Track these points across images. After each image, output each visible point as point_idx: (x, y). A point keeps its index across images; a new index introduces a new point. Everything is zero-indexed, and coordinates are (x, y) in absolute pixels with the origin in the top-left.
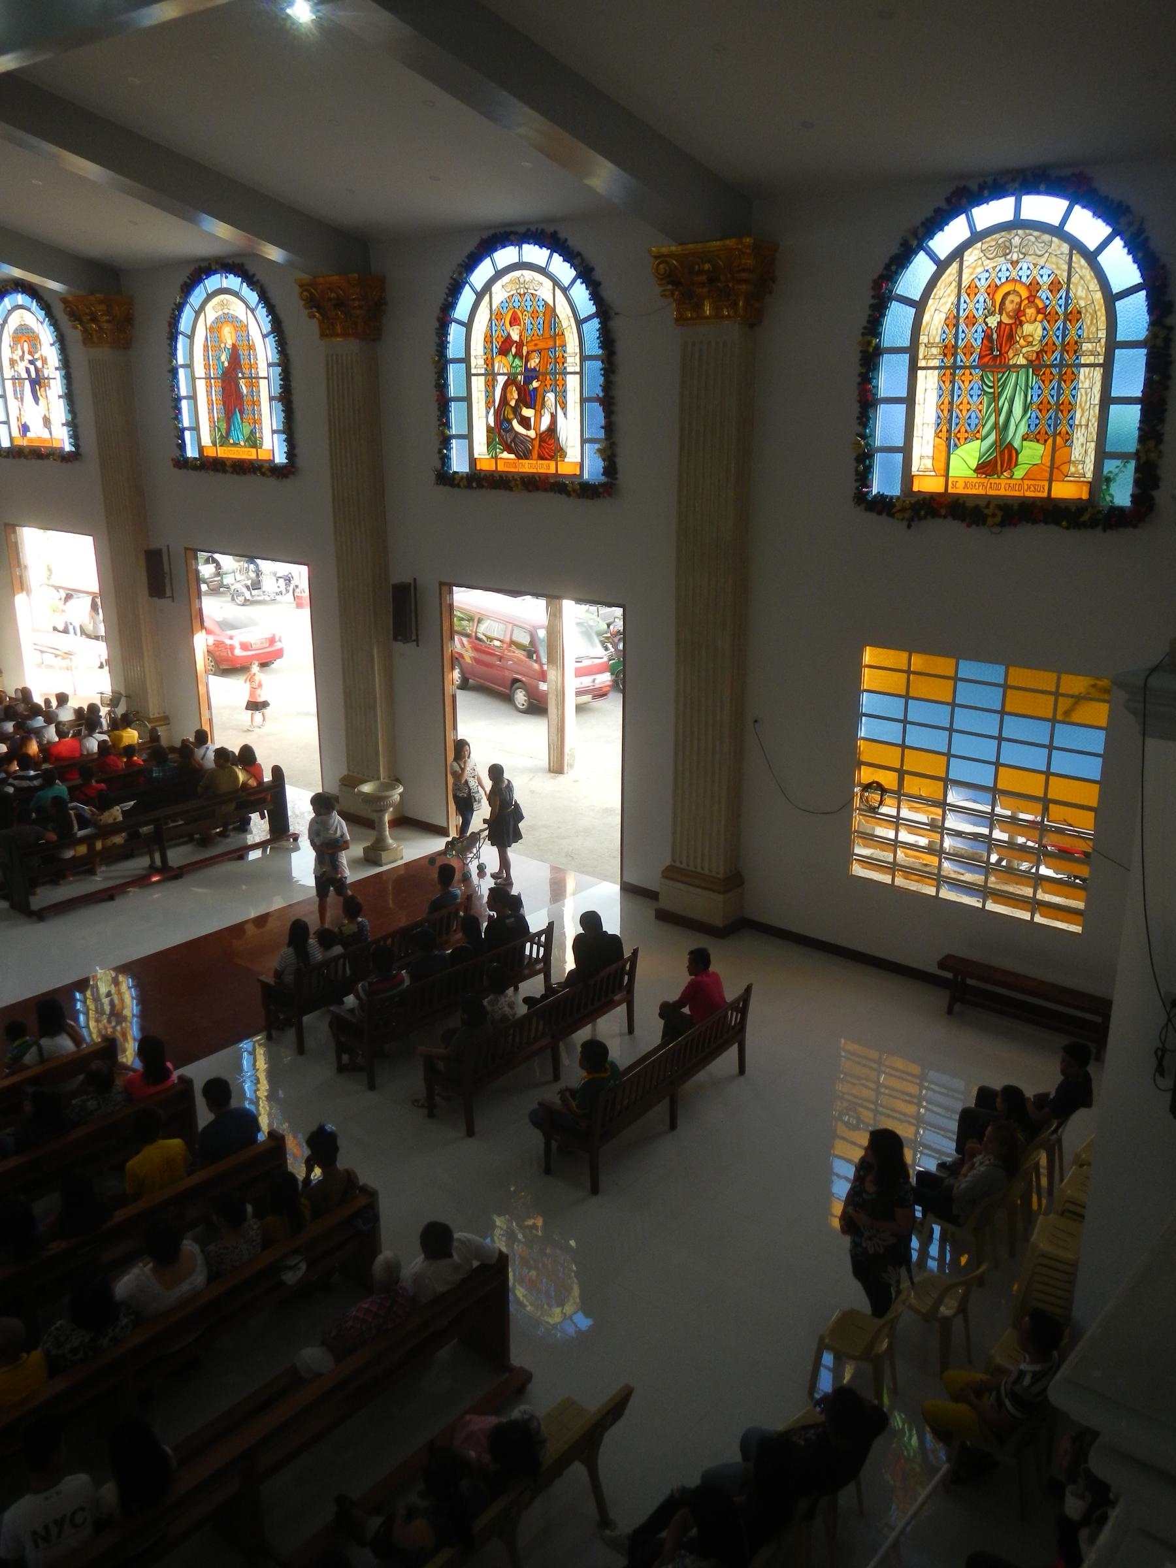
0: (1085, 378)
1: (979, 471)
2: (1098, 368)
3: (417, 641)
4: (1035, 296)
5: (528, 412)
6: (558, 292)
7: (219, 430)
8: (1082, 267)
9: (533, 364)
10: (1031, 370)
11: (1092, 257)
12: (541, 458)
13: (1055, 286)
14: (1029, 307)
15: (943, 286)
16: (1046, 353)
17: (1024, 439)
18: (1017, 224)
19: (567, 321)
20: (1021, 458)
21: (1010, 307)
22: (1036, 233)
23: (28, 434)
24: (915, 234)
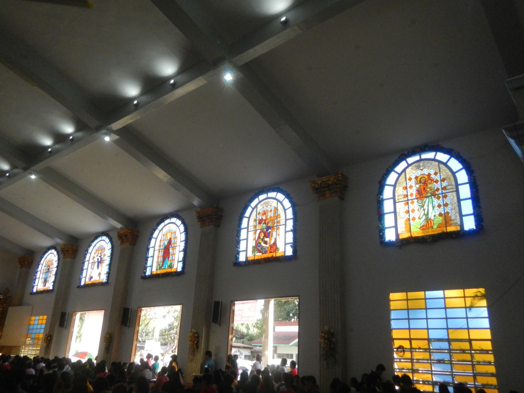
0: (451, 196)
1: (421, 228)
2: (454, 192)
3: (220, 324)
4: (430, 177)
5: (266, 239)
6: (279, 203)
7: (159, 265)
8: (443, 167)
9: (269, 225)
10: (433, 197)
11: (445, 164)
12: (270, 252)
13: (436, 174)
14: (429, 180)
15: (401, 180)
16: (436, 191)
17: (435, 216)
18: (421, 160)
19: (281, 210)
20: (435, 222)
21: (422, 181)
22: (427, 161)
23: (92, 280)
24: (390, 167)
